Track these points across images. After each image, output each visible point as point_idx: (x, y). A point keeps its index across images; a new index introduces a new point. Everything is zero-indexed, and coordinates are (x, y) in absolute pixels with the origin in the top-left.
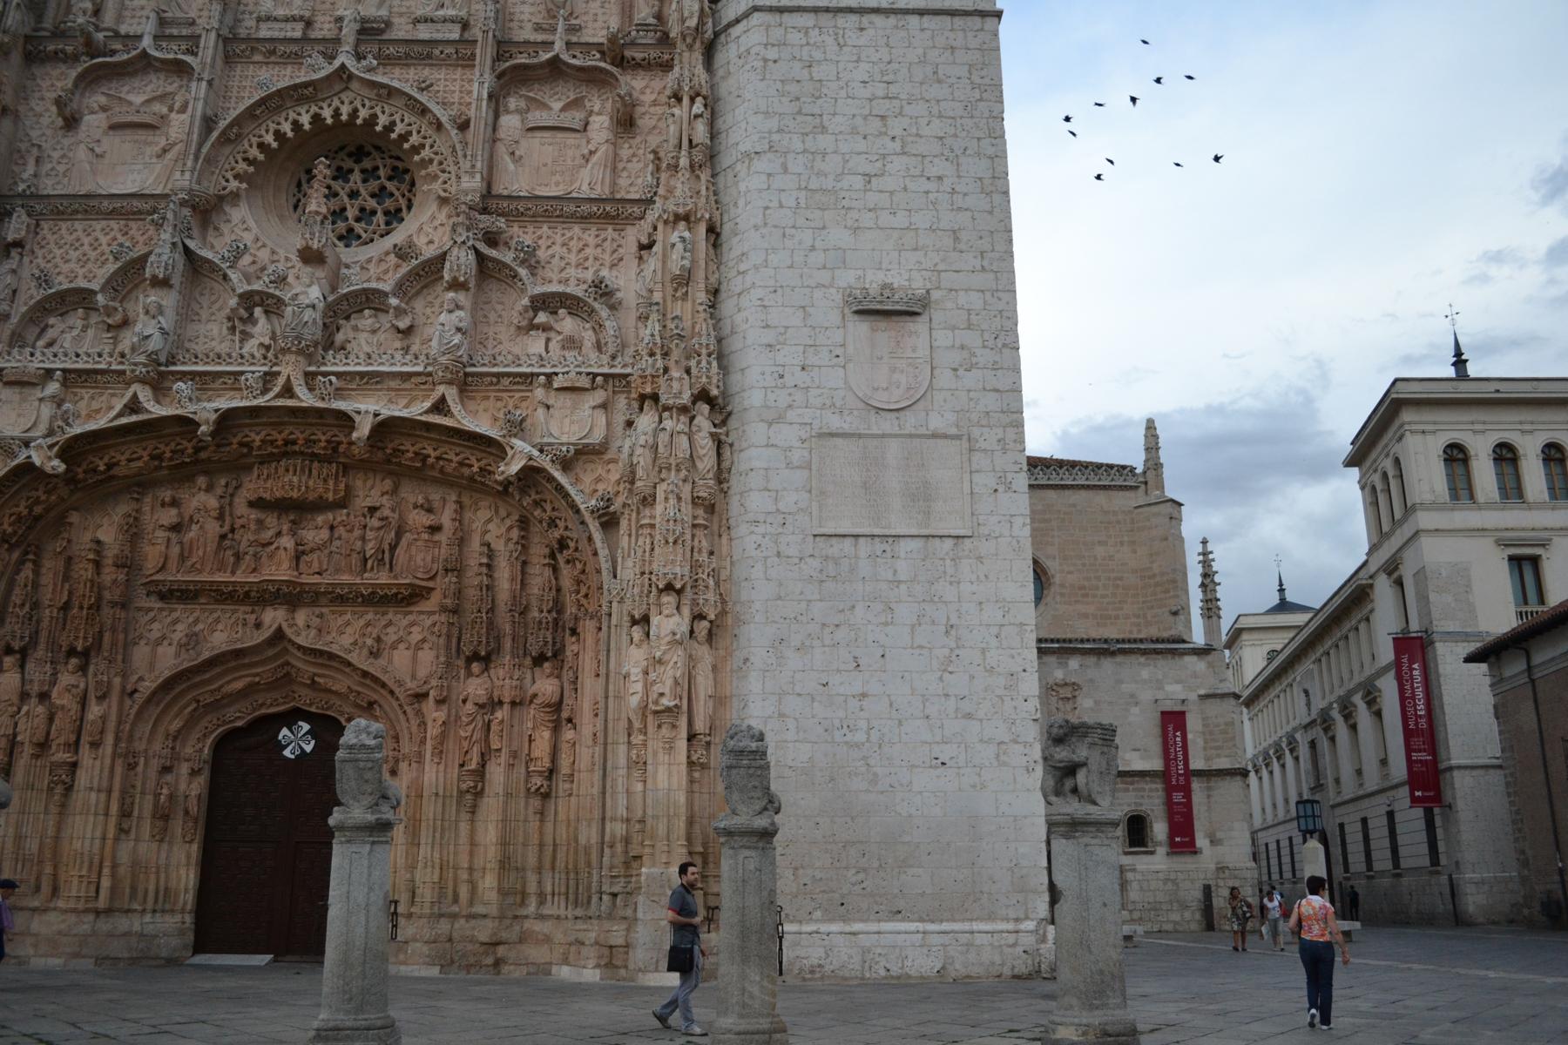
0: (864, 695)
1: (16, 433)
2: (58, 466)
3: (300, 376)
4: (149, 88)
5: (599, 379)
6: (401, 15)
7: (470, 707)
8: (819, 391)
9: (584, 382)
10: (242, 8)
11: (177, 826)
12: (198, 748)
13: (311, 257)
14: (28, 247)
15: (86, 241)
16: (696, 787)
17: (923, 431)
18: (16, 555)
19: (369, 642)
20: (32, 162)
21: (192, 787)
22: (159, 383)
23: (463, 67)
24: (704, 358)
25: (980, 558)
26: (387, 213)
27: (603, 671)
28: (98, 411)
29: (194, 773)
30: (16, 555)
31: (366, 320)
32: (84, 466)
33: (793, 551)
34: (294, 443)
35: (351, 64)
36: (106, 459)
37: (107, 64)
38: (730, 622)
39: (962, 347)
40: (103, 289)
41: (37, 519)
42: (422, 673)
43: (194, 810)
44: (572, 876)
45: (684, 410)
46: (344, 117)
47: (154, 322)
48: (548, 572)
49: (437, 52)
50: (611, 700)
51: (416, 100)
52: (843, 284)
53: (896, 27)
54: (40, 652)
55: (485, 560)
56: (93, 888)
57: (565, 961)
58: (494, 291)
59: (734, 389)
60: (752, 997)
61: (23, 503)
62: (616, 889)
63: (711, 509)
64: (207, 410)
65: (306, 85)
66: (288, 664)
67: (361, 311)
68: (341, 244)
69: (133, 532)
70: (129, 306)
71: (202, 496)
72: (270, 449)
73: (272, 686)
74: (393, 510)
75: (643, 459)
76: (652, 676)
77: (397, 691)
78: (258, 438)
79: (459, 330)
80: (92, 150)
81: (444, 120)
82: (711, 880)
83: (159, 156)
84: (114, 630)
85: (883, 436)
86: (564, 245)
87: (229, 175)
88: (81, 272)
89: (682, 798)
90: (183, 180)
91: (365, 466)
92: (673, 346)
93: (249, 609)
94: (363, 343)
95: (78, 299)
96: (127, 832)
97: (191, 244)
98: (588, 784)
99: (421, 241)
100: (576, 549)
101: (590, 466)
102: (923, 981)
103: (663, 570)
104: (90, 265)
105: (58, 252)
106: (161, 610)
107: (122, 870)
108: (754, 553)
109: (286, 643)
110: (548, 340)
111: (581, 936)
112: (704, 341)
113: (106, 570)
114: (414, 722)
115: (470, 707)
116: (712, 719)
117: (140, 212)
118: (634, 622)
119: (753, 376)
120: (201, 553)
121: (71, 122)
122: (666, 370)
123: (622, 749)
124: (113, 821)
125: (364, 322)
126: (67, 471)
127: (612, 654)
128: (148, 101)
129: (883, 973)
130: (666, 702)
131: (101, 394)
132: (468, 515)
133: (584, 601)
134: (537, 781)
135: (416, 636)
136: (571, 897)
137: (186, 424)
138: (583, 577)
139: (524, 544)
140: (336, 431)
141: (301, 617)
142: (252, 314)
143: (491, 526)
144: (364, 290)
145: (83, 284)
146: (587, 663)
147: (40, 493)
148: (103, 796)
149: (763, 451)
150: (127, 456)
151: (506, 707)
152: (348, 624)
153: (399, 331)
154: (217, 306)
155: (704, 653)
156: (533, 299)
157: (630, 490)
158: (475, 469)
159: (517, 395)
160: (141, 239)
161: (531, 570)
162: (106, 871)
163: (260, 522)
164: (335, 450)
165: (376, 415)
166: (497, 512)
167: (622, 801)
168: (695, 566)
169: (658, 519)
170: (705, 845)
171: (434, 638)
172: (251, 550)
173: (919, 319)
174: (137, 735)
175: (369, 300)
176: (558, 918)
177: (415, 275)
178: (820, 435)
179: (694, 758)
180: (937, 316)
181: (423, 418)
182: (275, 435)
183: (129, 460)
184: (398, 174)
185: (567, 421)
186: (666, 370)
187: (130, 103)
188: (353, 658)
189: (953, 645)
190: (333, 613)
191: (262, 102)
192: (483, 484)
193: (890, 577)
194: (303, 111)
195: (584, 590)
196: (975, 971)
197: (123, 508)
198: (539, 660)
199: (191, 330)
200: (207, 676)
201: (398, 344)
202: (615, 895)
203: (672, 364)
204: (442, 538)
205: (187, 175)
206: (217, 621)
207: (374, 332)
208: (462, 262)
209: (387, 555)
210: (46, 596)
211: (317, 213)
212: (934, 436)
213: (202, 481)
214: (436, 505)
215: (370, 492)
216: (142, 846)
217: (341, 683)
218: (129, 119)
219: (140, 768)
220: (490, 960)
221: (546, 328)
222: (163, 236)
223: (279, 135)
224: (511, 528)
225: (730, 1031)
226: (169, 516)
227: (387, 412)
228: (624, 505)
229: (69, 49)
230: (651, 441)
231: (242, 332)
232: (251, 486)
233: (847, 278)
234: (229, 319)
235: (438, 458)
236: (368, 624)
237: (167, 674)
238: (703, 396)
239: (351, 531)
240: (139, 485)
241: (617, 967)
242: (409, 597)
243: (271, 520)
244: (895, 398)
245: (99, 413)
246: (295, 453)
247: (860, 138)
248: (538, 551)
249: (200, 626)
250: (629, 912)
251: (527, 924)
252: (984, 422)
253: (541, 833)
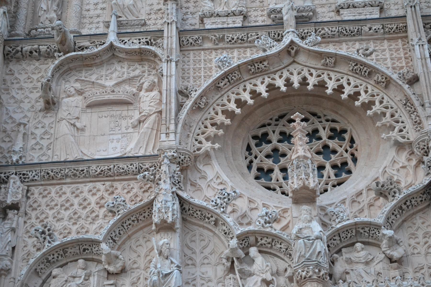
4: (114, 75)
6: (322, 6)
10: (184, 10)
13: (305, 197)
14: (22, 209)
15: (76, 201)
20: (20, 136)
23: (389, 39)
26: (334, 167)
31: (360, 252)
35: (297, 40)
37: (76, 57)
46: (296, 85)
47: (168, 262)
49: (366, 29)
51: (364, 64)
65: (261, 60)
67: (353, 244)
80: (74, 125)
81: (395, 77)
83: (134, 127)
87: (201, 138)
90: (170, 141)
94: (363, 274)
95: (84, 249)
97: (180, 193)
104: (81, 222)
105: (51, 213)
117: (126, 173)
121: (50, 105)
125: (356, 255)
128: (118, 84)
142: (247, 254)
144: (356, 224)
153: (391, 260)
154: (207, 251)
175: (360, 234)
177: (399, 208)
184: (337, 134)
187: (104, 87)
191: (225, 76)
194: (259, 83)
201: (396, 273)
205: (172, 136)
207: (367, 263)
211: (306, 158)
218: (107, 97)
222: (163, 186)
223: (240, 103)
229: (43, 48)
231: (240, 271)
234: (228, 259)
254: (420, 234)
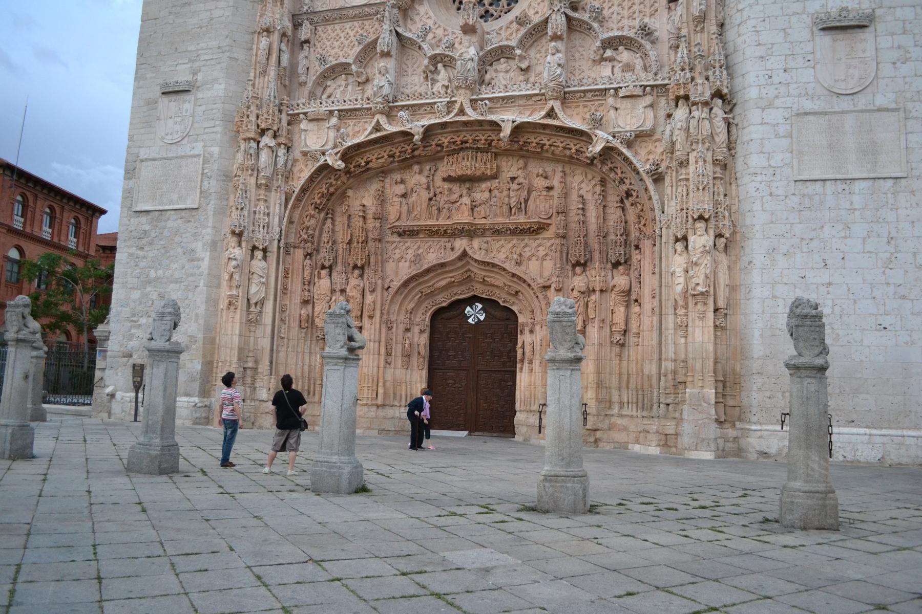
0: (830, 284)
1: (317, 148)
2: (340, 164)
3: (468, 102)
5: (648, 88)
7: (575, 293)
8: (795, 86)
9: (639, 91)
11: (415, 360)
12: (423, 319)
13: (468, 30)
16: (718, 341)
17: (871, 107)
18: (322, 215)
19: (515, 256)
21: (422, 340)
22: (390, 112)
24: (717, 69)
25: (913, 192)
27: (657, 270)
28: (359, 132)
29: (421, 332)
30: (322, 215)
31: (502, 65)
32: (354, 164)
33: (781, 192)
34: (466, 142)
36: (365, 159)
38: (738, 239)
39: (899, 47)
40: (354, 62)
41: (332, 194)
42: (546, 274)
43: (423, 352)
44: (640, 392)
45: (706, 104)
48: (619, 211)
50: (663, 288)
52: (812, 11)
54: (339, 268)
55: (581, 206)
56: (375, 393)
57: (637, 441)
58: (577, 39)
59: (737, 89)
60: (813, 470)
61: (324, 187)
62: (668, 401)
63: (725, 167)
64: (417, 126)
66: (469, 270)
68: (482, 21)
69: (382, 199)
70: (369, 70)
71: (417, 177)
72: (453, 147)
73: (461, 283)
74: (525, 179)
75: (679, 137)
76: (691, 273)
77: (532, 284)
78: (446, 141)
79: (559, 65)
82: (728, 398)
84: (376, 254)
85: (842, 112)
86: (619, 5)
88: (341, 53)
89: (711, 348)
91: (507, 153)
92: (697, 63)
93: (447, 240)
94: (502, 80)
95: (343, 68)
96: (389, 364)
97: (400, 30)
98: (649, 339)
99: (531, 13)
100: (637, 197)
101: (644, 144)
102: (868, 466)
103: (696, 207)
104: (345, 49)
105: (328, 44)
106: (400, 242)
107: (388, 384)
108: (755, 194)
109: (468, 259)
110: (613, 67)
111: (647, 427)
112: (717, 58)
113: (369, 221)
114: (543, 303)
115: (575, 293)
116: (728, 299)
117: (370, 15)
118: (677, 240)
119: (751, 78)
120: (419, 209)
122: (693, 79)
123: (671, 318)
124: (382, 358)
126: (346, 167)
127: (663, 260)
129: (841, 458)
130: (700, 289)
131: (359, 123)
132: (569, 179)
133: (643, 228)
134: (617, 337)
135: (541, 253)
136: (640, 405)
137: (407, 135)
138: (642, 214)
139: (604, 194)
140: (490, 133)
141: (476, 243)
142: (436, 68)
143: (583, 185)
145: (344, 60)
146: (647, 267)
147: (332, 180)
148: (377, 344)
149: (760, 129)
150: (376, 156)
151: (597, 293)
152: (502, 246)
153: (522, 70)
155: (722, 258)
156: (603, 42)
157: (671, 158)
158: (573, 151)
159: (597, 103)
160: (371, 31)
161: (608, 210)
162: (381, 384)
163: (450, 190)
164: (490, 145)
165: (513, 122)
166: (586, 177)
167: (671, 349)
168: (716, 203)
169: (691, 175)
170: (724, 376)
171: (552, 253)
172: (446, 206)
173: (867, 30)
174: (392, 312)
175: (503, 53)
176: (632, 416)
177: (529, 34)
178: (798, 115)
179: (717, 323)
180: (880, 27)
181: (541, 122)
182: (456, 139)
183: (377, 159)
185: (629, 117)
186: (693, 79)
188: (507, 266)
189: (893, 250)
190: (494, 240)
192: (578, 159)
193: (848, 206)
195: (643, 222)
196: (904, 460)
197: (374, 186)
198: (616, 265)
199: (404, 81)
200: (426, 278)
201: (522, 78)
202: (668, 405)
203: (696, 75)
204: (554, 193)
206: (430, 247)
207: (507, 72)
208: (558, 22)
209: (523, 205)
210: (339, 237)
212: (880, 110)
213: (416, 168)
214: (550, 174)
215: (510, 168)
216: (397, 371)
217: (499, 280)
219: (394, 330)
220: (592, 439)
221: (611, 59)
222: (384, 27)
224: (595, 185)
225: (799, 490)
226: (400, 189)
227: (519, 120)
228: (668, 167)
230: (685, 125)
231: (432, 79)
232: (444, 169)
233: (814, 7)
234: (424, 72)
235: (550, 146)
236: (514, 246)
237: (405, 278)
238: (718, 94)
239: (501, 192)
240: (383, 172)
241: (670, 447)
242: (536, 230)
243: (456, 188)
244: (851, 86)
245: (360, 132)
246: (467, 148)
248: (613, 199)
249: (421, 251)
250: (677, 415)
251: (613, 420)
252: (915, 98)
253: (620, 368)
254: (543, 50)
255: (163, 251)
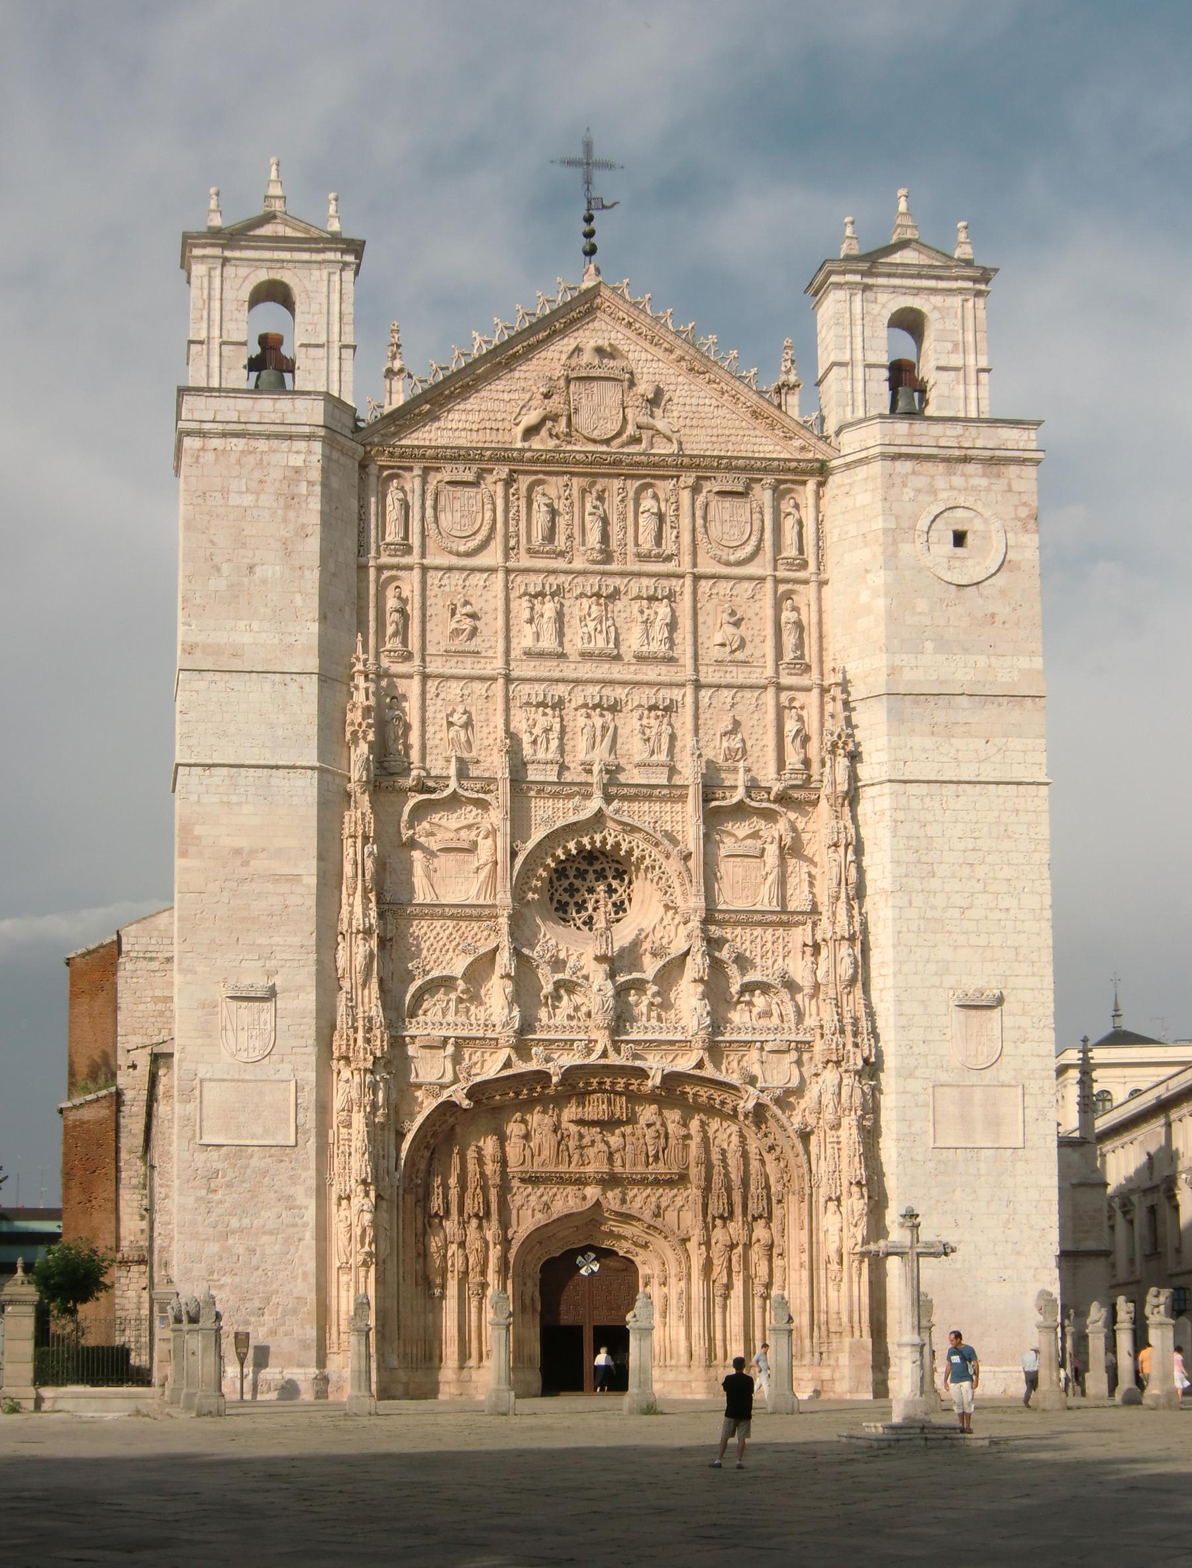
46: (598, 844)
49: (656, 792)
53: (981, 794)
209: (661, 1153)
247: (957, 880)
255: (248, 1195)
